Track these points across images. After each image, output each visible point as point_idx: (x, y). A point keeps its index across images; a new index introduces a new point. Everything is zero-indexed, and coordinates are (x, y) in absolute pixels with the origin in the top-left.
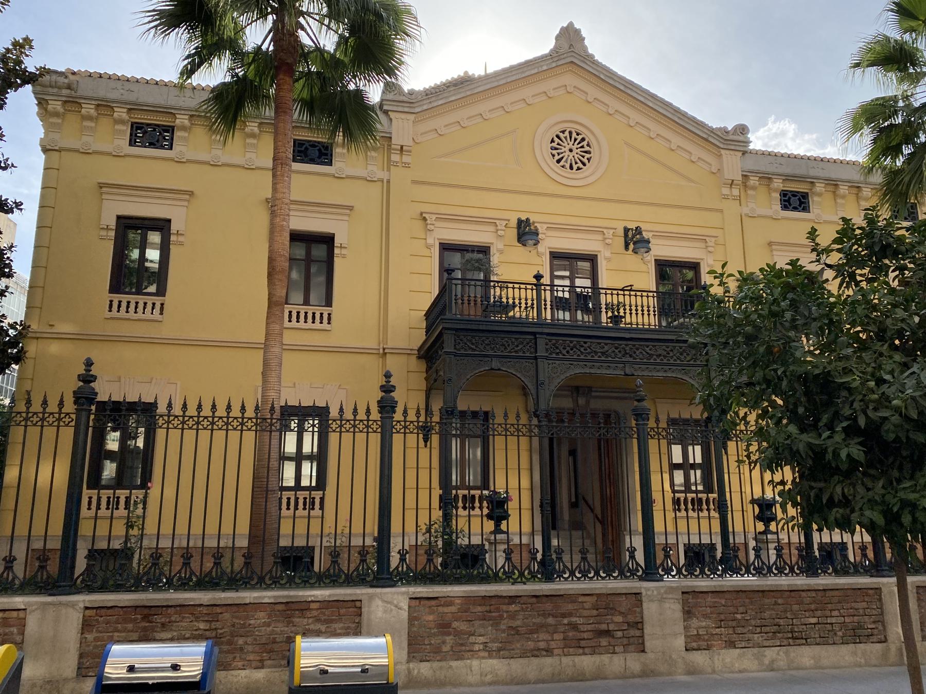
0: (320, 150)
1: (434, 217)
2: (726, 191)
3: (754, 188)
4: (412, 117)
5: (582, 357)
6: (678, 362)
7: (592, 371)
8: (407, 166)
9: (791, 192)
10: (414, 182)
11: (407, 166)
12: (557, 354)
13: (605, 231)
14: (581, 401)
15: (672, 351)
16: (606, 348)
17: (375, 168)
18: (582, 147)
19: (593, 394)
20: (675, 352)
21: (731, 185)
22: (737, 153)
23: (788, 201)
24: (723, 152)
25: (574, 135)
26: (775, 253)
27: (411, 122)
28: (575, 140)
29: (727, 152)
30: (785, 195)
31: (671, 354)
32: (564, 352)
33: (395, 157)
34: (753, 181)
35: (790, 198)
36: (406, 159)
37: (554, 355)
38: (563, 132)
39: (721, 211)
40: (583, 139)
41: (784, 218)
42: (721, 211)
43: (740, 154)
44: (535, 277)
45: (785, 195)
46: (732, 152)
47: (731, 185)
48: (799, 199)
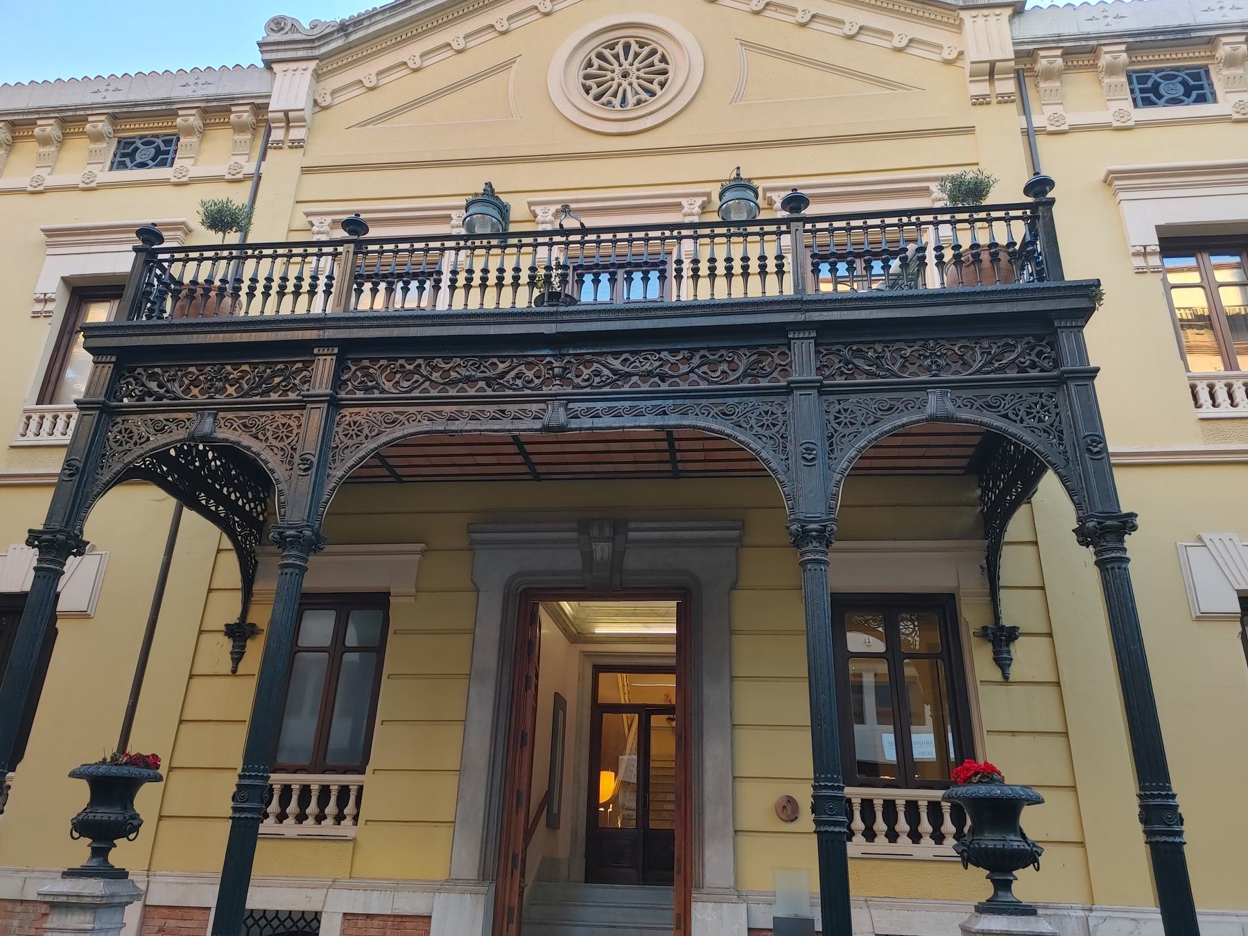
0: (158, 149)
1: (329, 219)
2: (982, 88)
3: (1049, 75)
4: (312, 65)
5: (434, 393)
6: (704, 386)
7: (454, 426)
8: (297, 145)
9: (1157, 71)
10: (306, 170)
11: (297, 145)
12: (367, 390)
13: (684, 201)
14: (602, 550)
15: (687, 360)
16: (502, 367)
17: (242, 160)
18: (637, 55)
19: (632, 535)
20: (696, 361)
21: (991, 73)
22: (998, 11)
23: (1155, 89)
24: (963, 14)
25: (634, 47)
26: (1122, 195)
27: (309, 73)
28: (637, 55)
29: (974, 13)
30: (1142, 80)
31: (684, 369)
32: (388, 386)
33: (277, 135)
34: (1049, 60)
35: (1156, 85)
36: (296, 134)
37: (360, 394)
38: (612, 47)
39: (970, 130)
40: (653, 52)
41: (1140, 125)
42: (970, 130)
43: (1009, 11)
44: (346, 225)
45: (1142, 80)
46: (986, 12)
47: (991, 73)
48: (1184, 83)
